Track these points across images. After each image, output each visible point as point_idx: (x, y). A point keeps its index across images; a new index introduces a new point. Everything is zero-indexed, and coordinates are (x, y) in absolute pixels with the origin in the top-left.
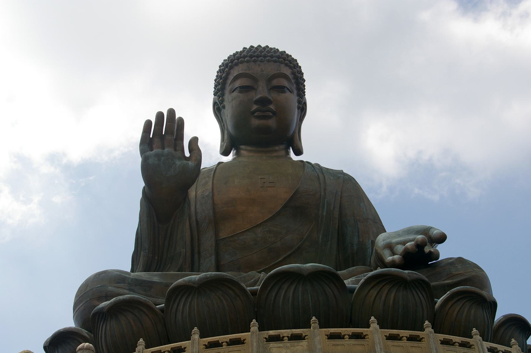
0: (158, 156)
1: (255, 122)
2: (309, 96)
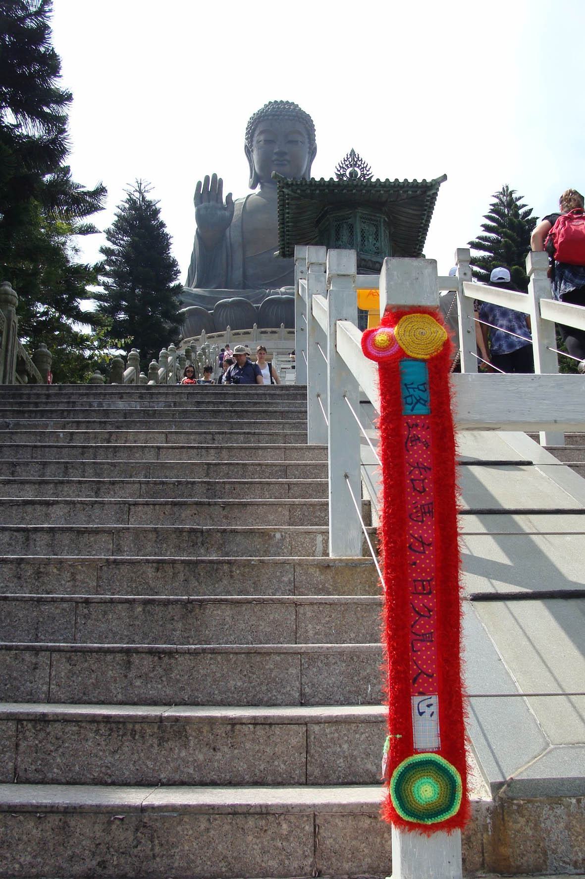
0: (206, 208)
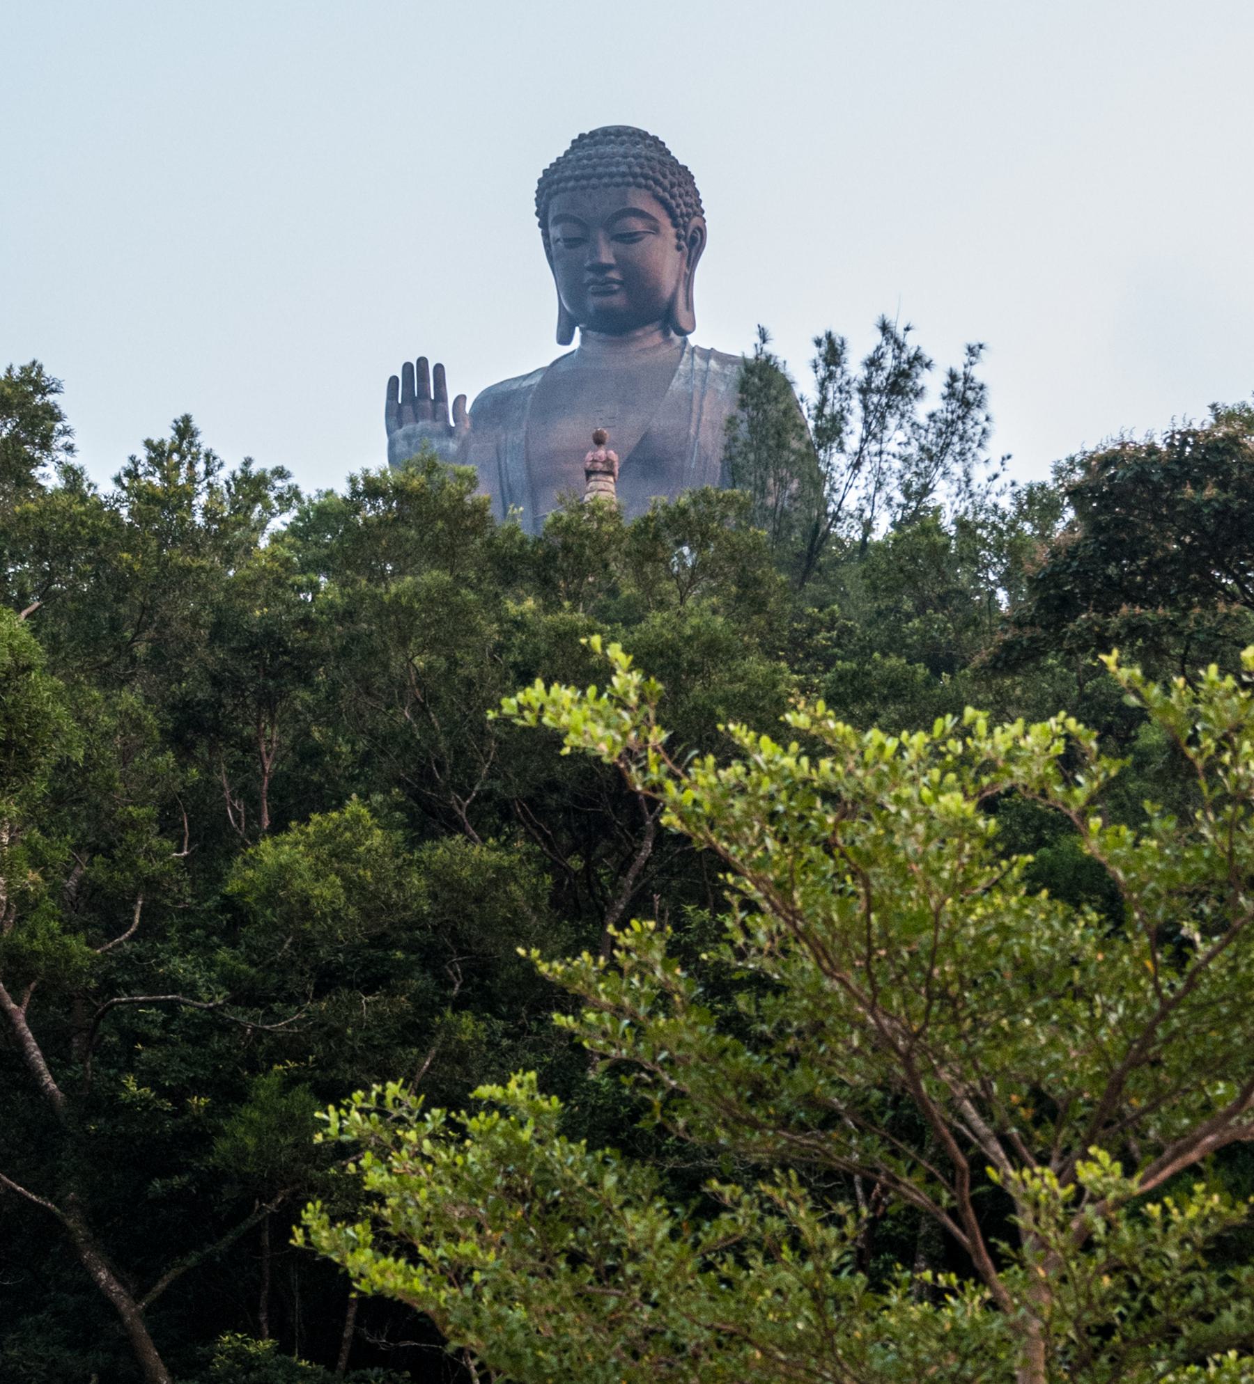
0: (408, 437)
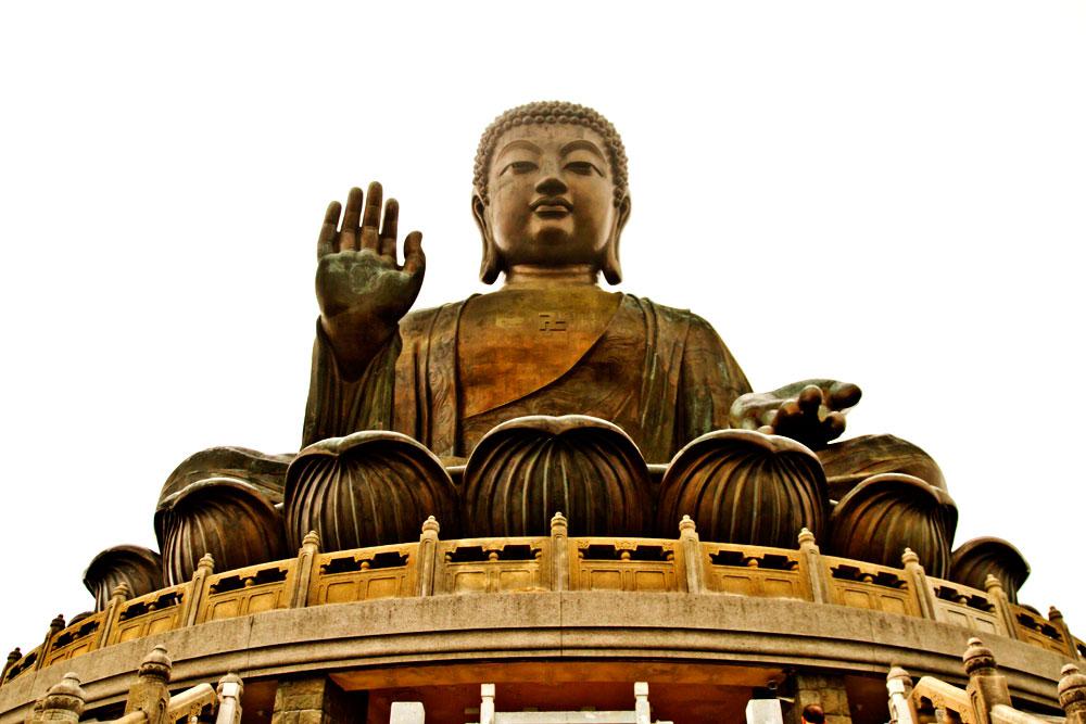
0: (346, 261)
1: (536, 226)
2: (635, 188)
